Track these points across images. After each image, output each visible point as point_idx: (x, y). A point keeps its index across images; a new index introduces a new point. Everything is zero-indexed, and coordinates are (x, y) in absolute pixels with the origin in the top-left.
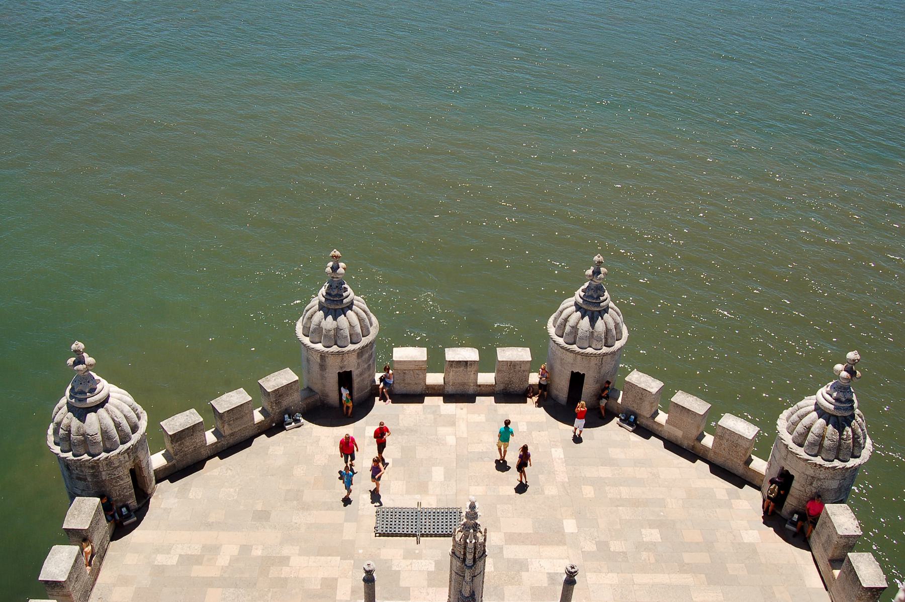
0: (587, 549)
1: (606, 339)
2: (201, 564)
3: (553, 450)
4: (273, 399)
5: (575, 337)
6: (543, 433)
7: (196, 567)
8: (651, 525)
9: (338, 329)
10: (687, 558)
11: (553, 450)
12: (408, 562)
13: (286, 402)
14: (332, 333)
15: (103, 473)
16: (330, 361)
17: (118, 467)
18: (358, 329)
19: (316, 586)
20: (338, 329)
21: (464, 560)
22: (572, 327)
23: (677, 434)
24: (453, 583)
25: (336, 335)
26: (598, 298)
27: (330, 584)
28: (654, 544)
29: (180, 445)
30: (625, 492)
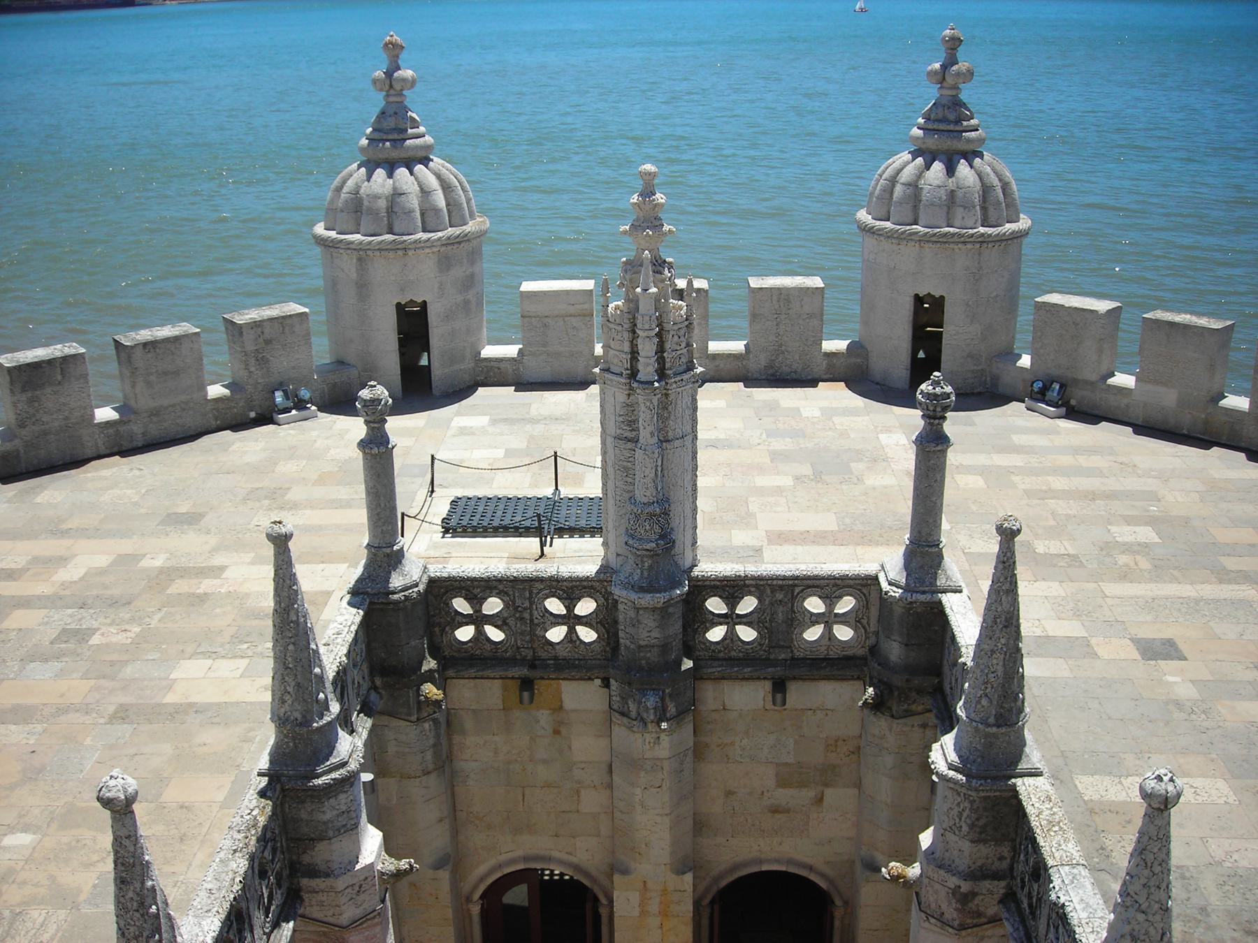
1: (984, 209)
4: (250, 347)
5: (915, 208)
6: (860, 419)
8: (1130, 521)
9: (397, 194)
10: (1231, 563)
13: (281, 363)
14: (382, 204)
16: (381, 270)
18: (440, 200)
20: (397, 194)
21: (633, 374)
22: (908, 185)
23: (1167, 399)
24: (610, 470)
25: (391, 210)
26: (958, 122)
28: (1146, 545)
29: (31, 401)
30: (1058, 483)
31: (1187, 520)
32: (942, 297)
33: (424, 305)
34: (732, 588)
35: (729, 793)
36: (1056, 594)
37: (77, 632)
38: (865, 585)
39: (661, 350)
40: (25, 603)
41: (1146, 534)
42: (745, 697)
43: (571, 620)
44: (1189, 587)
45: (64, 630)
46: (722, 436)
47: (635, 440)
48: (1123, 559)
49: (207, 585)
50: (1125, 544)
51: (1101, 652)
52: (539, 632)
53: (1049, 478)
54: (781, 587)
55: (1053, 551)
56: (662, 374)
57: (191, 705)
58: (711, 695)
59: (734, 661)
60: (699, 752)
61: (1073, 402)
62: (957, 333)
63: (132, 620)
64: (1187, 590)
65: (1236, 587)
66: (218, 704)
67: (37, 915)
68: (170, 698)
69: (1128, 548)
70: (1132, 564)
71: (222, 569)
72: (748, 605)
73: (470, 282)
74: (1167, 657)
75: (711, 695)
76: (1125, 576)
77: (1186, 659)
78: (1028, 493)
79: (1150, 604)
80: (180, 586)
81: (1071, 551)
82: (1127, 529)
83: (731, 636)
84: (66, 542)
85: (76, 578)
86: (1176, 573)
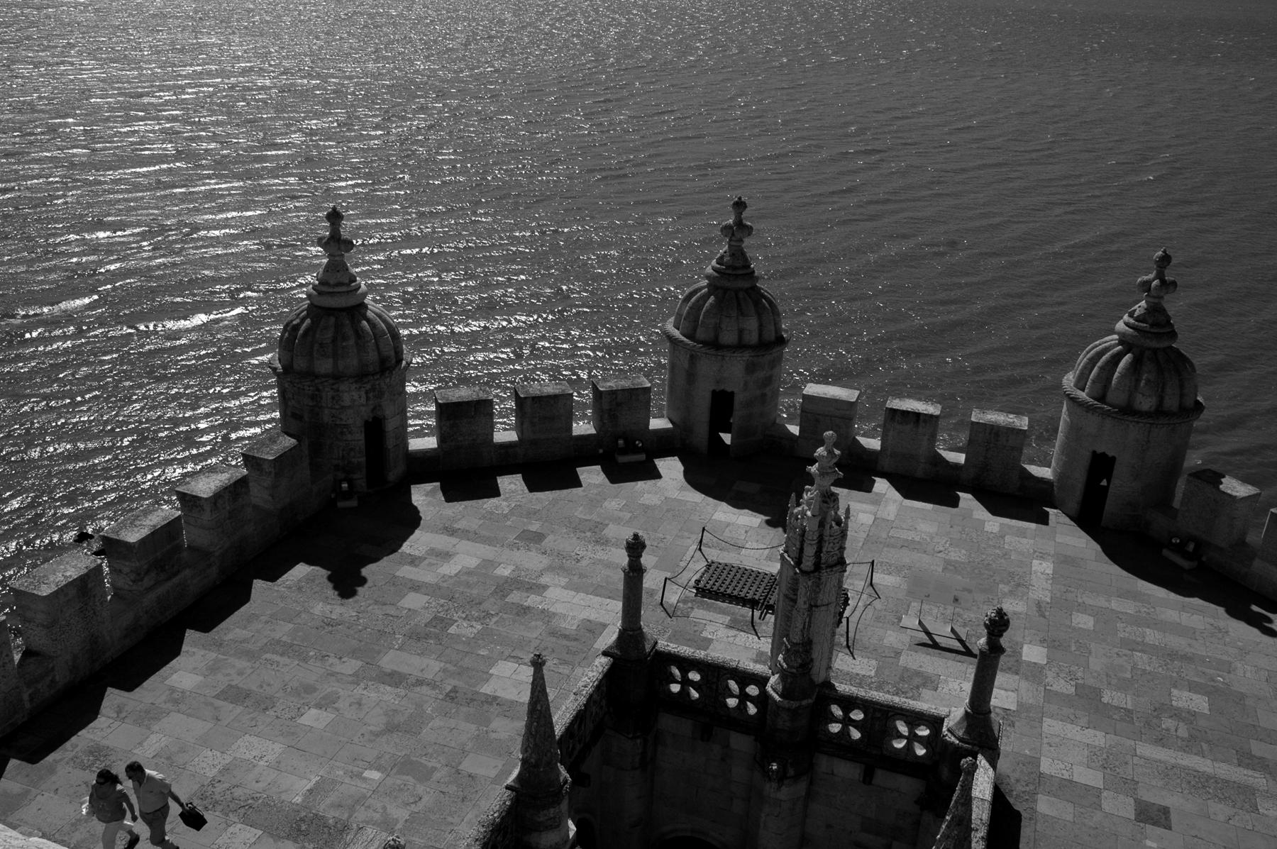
0: (1055, 688)
2: (416, 566)
3: (1035, 562)
4: (606, 407)
6: (1024, 541)
7: (407, 568)
8: (1193, 687)
10: (1257, 748)
11: (1035, 562)
12: (732, 632)
15: (326, 411)
17: (349, 407)
19: (570, 626)
27: (594, 629)
28: (1194, 714)
30: (1152, 636)
31: (1243, 697)
32: (1114, 459)
33: (731, 395)
34: (849, 703)
35: (829, 826)
36: (1097, 743)
37: (442, 620)
38: (936, 722)
39: (819, 551)
40: (416, 587)
41: (1200, 703)
42: (847, 770)
43: (744, 697)
44: (1209, 762)
45: (435, 618)
46: (917, 539)
47: (795, 601)
48: (1168, 723)
49: (532, 600)
50: (1178, 709)
51: (1106, 806)
52: (721, 698)
53: (1148, 630)
54: (880, 710)
55: (1115, 703)
56: (817, 567)
57: (495, 698)
58: (824, 763)
59: (841, 746)
60: (810, 795)
61: (1204, 559)
62: (1121, 486)
63: (478, 619)
64: (1205, 765)
65: (1250, 772)
66: (512, 702)
67: (370, 831)
68: (487, 689)
69: (1177, 714)
70: (1173, 729)
71: (545, 587)
72: (857, 715)
73: (768, 381)
74: (1156, 823)
75: (824, 763)
76: (1161, 741)
77: (1170, 829)
78: (1125, 643)
79: (1168, 773)
80: (515, 597)
81: (1129, 707)
82: (1186, 694)
83: (844, 733)
84: (454, 540)
85: (454, 572)
86: (1205, 746)
